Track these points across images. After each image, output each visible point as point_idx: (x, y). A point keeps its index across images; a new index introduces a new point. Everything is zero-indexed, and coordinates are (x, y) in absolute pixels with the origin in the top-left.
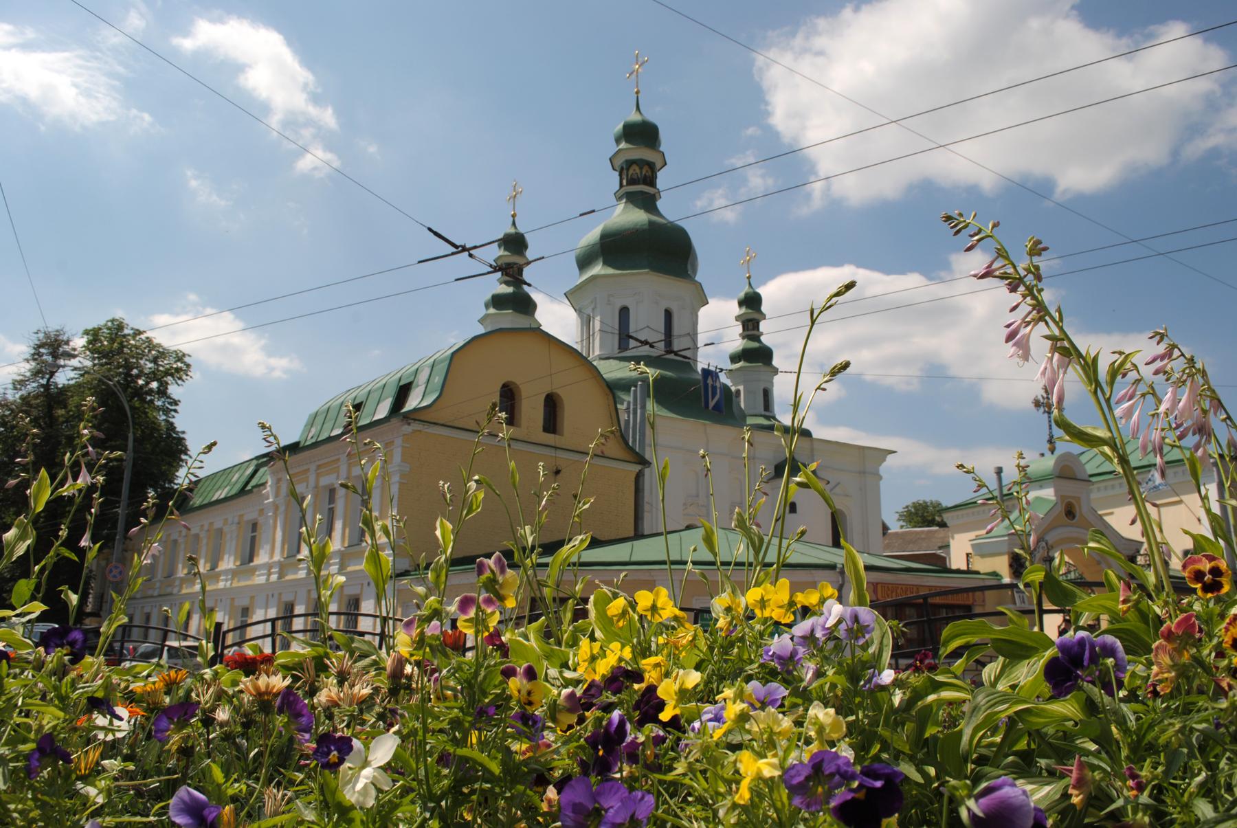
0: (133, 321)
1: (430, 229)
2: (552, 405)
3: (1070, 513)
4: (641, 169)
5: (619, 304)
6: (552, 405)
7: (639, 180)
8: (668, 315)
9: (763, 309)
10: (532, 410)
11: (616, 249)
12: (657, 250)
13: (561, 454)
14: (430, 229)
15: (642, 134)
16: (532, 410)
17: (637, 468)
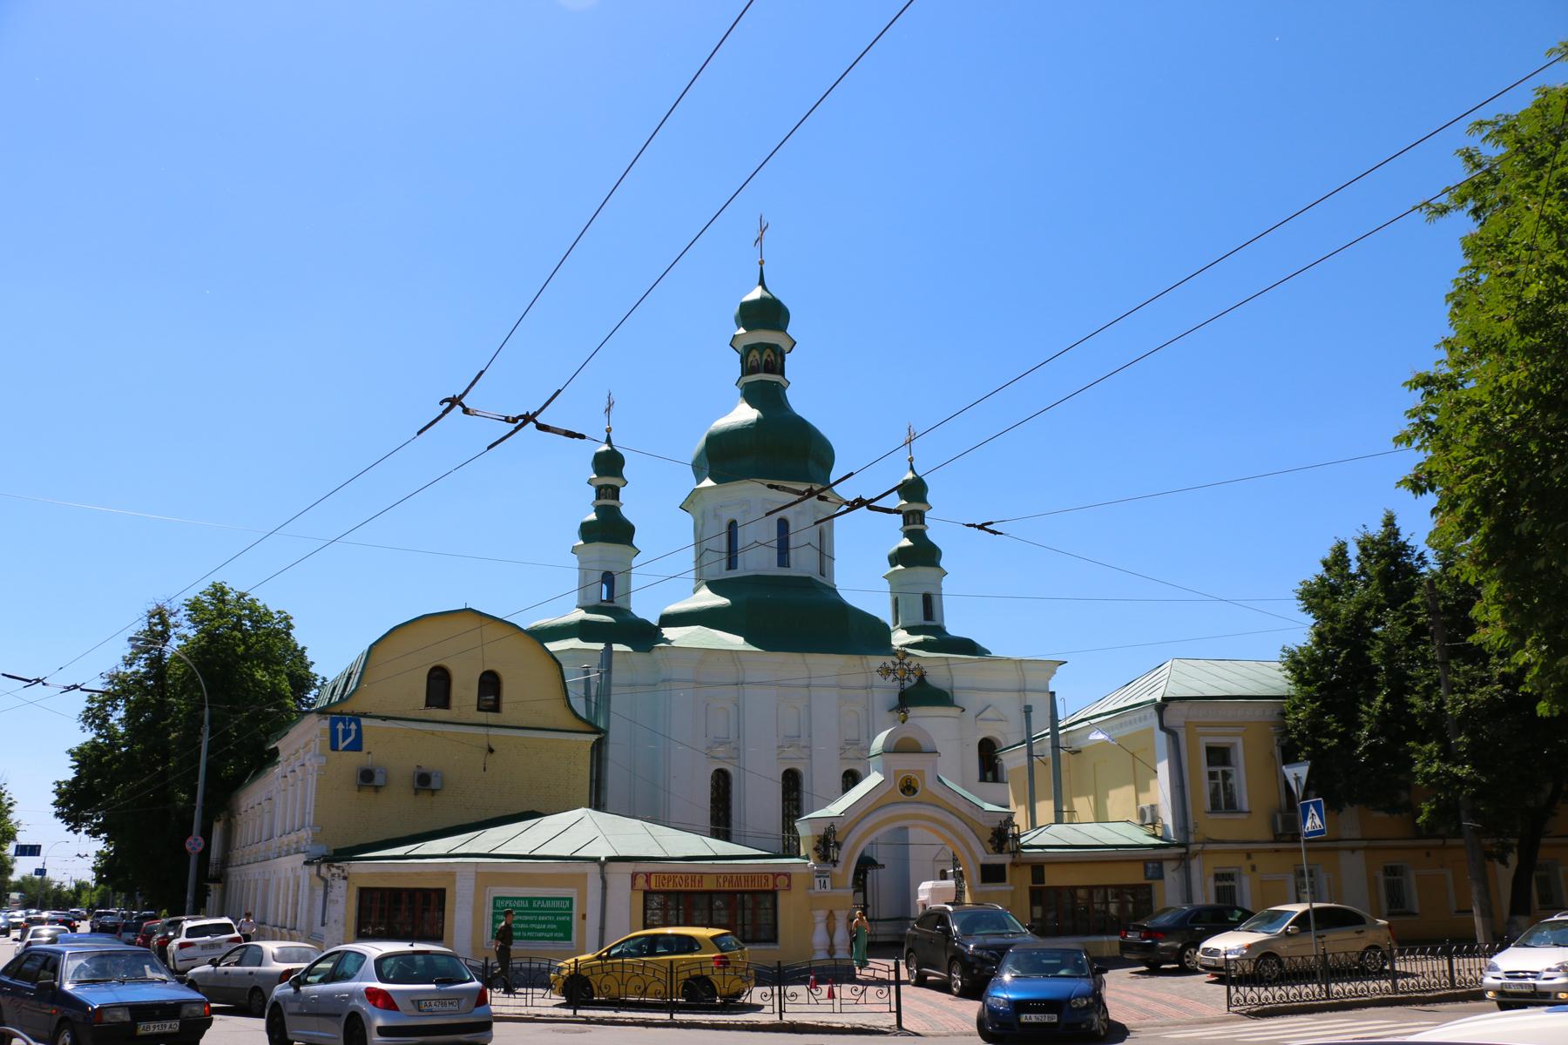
0: (237, 582)
1: (582, 437)
2: (490, 684)
3: (908, 788)
4: (761, 354)
5: (727, 516)
6: (490, 684)
7: (763, 371)
8: (783, 525)
9: (929, 498)
10: (465, 690)
11: (724, 456)
12: (776, 451)
13: (493, 731)
14: (582, 437)
15: (766, 315)
16: (465, 690)
17: (594, 737)
